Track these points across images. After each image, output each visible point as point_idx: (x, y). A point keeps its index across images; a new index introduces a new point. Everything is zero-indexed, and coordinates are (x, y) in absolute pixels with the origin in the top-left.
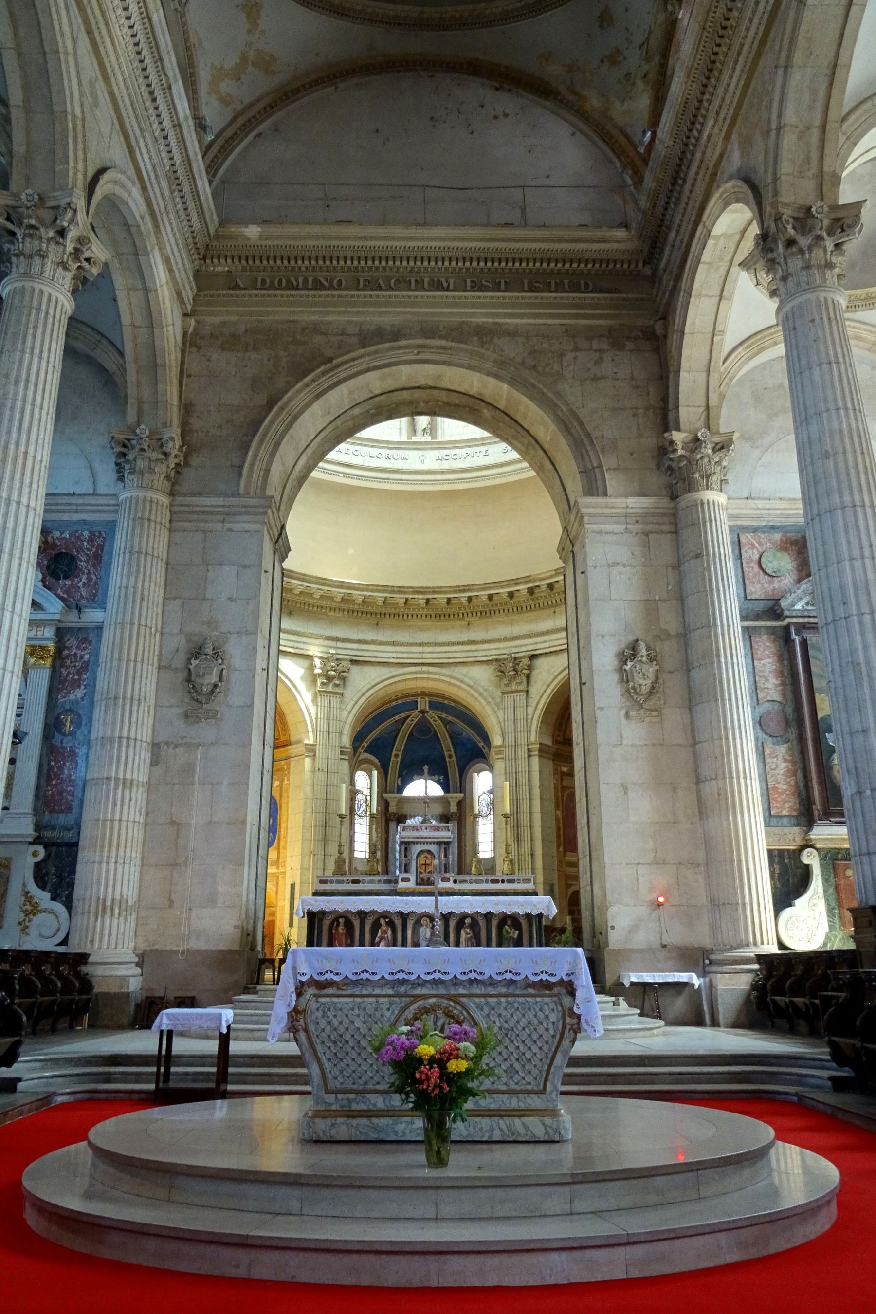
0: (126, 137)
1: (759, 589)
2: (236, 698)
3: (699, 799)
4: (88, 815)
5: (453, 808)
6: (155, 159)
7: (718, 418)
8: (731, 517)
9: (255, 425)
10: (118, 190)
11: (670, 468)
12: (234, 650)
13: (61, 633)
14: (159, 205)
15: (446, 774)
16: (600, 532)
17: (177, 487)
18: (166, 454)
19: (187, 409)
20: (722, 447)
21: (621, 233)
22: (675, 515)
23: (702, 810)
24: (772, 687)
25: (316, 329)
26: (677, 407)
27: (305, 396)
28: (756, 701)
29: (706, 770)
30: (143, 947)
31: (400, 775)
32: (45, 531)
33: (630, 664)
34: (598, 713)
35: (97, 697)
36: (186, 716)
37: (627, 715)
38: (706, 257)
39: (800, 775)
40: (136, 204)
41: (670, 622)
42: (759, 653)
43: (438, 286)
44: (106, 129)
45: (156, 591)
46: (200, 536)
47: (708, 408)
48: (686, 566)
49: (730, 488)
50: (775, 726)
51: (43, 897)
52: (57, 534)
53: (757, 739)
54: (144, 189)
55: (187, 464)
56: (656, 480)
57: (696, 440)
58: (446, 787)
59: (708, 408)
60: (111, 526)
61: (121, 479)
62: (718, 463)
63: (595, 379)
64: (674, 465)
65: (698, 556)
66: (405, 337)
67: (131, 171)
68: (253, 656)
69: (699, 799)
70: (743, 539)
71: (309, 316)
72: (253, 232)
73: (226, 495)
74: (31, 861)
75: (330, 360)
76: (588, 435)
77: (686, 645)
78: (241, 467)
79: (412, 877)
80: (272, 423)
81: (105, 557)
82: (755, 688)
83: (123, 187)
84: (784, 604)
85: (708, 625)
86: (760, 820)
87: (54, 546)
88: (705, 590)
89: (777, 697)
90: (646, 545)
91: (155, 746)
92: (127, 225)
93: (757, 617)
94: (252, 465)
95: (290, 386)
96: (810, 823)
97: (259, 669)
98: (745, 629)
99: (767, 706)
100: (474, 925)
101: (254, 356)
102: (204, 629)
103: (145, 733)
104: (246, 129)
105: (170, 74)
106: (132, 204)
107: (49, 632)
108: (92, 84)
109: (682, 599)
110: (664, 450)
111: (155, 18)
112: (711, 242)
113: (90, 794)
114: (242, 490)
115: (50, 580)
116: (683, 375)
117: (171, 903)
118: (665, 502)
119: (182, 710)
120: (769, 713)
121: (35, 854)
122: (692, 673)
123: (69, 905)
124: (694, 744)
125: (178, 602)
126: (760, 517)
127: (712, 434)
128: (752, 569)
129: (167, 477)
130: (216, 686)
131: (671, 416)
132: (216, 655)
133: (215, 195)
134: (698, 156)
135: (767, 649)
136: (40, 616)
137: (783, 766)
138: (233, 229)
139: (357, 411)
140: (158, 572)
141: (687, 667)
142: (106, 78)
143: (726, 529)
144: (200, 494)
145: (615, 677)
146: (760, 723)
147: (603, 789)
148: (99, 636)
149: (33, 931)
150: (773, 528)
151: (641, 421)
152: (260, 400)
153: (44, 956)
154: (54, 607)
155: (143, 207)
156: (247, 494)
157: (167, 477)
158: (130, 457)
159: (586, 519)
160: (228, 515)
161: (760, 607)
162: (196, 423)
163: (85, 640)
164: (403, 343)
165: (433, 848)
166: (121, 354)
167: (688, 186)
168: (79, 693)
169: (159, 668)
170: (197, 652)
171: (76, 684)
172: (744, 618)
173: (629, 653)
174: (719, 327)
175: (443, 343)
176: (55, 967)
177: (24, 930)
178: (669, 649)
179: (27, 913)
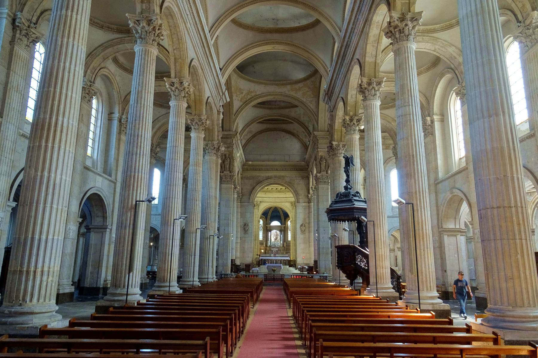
5: (283, 229)
9: (251, 192)
12: (250, 225)
15: (281, 221)
19: (242, 189)
21: (303, 162)
23: (309, 247)
25: (260, 176)
27: (258, 187)
31: (270, 220)
41: (307, 221)
43: (277, 170)
56: (307, 200)
58: (281, 224)
63: (299, 184)
72: (250, 163)
75: (261, 181)
80: (254, 192)
91: (240, 238)
100: (280, 261)
104: (248, 143)
110: (308, 196)
118: (307, 204)
138: (248, 162)
152: (252, 188)
162: (243, 191)
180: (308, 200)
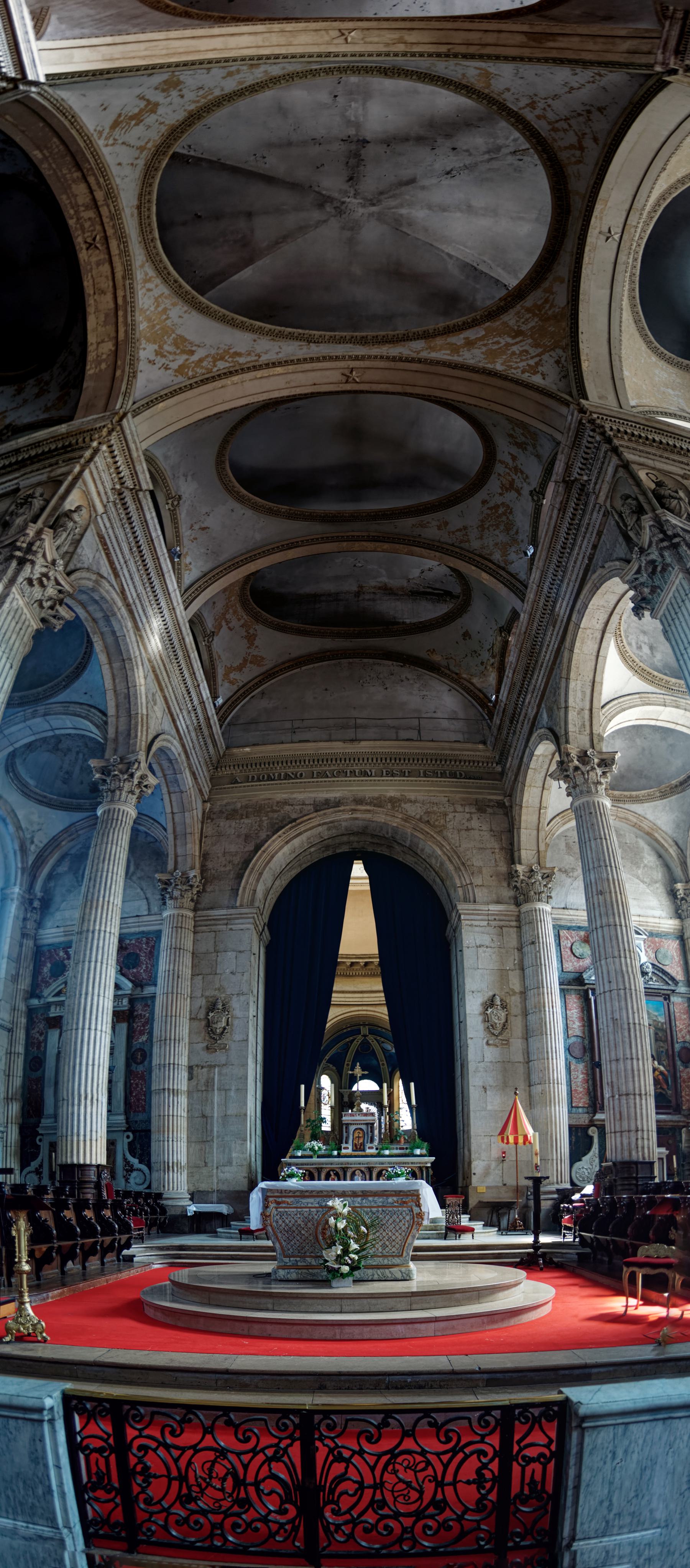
0: (172, 715)
1: (571, 965)
2: (237, 1037)
3: (530, 1095)
4: (154, 1113)
6: (188, 722)
7: (545, 857)
8: (554, 919)
10: (165, 744)
11: (516, 887)
13: (132, 1001)
14: (189, 745)
16: (471, 925)
17: (199, 906)
18: (192, 886)
20: (548, 877)
22: (519, 916)
24: (577, 1027)
26: (519, 850)
28: (567, 1036)
29: (534, 1078)
30: (192, 1189)
32: (121, 940)
33: (490, 1010)
34: (469, 1041)
35: (155, 1040)
36: (207, 1048)
37: (488, 1044)
38: (532, 765)
39: (590, 1082)
40: (176, 748)
42: (569, 1006)
44: (159, 714)
45: (187, 972)
46: (213, 934)
47: (538, 851)
48: (525, 949)
49: (553, 902)
50: (577, 1052)
51: (135, 1161)
52: (128, 942)
53: (566, 1059)
54: (181, 739)
55: (204, 890)
57: (532, 871)
59: (538, 851)
60: (158, 934)
61: (164, 904)
62: (545, 886)
64: (518, 885)
65: (533, 943)
66: (343, 804)
67: (174, 732)
68: (247, 1009)
69: (530, 1095)
70: (561, 933)
71: (281, 796)
73: (228, 908)
74: (126, 1141)
76: (463, 864)
77: (525, 999)
78: (238, 890)
79: (350, 1147)
81: (156, 953)
82: (567, 1028)
83: (169, 741)
84: (585, 976)
85: (539, 986)
86: (565, 1109)
87: (126, 948)
88: (538, 965)
89: (579, 1033)
90: (501, 935)
92: (170, 761)
93: (569, 984)
94: (245, 888)
95: (269, 837)
96: (595, 1113)
97: (251, 1017)
98: (562, 990)
99: (573, 1040)
101: (246, 821)
102: (216, 993)
103: (184, 1061)
105: (199, 679)
106: (173, 749)
107: (125, 1002)
108: (153, 695)
109: (522, 969)
110: (511, 875)
111: (192, 656)
112: (534, 758)
113: (155, 1100)
114: (238, 904)
115: (125, 970)
116: (523, 831)
117: (206, 1164)
119: (205, 1045)
120: (574, 1043)
121: (128, 1137)
122: (529, 1017)
123: (149, 1166)
124: (528, 1062)
125: (200, 977)
126: (571, 920)
127: (541, 868)
128: (567, 953)
129: (192, 900)
130: (224, 1029)
131: (516, 854)
132: (224, 1008)
133: (223, 734)
134: (524, 711)
135: (574, 1002)
136: (120, 993)
137: (581, 1076)
139: (312, 850)
140: (188, 960)
141: (525, 1014)
142: (162, 690)
143: (551, 927)
144: (212, 908)
145: (480, 1018)
146: (569, 1050)
147: (471, 1089)
148: (153, 1002)
149: (132, 1181)
150: (580, 928)
151: (497, 856)
153: (138, 1194)
154: (128, 985)
155: (180, 749)
156: (241, 906)
157: (192, 900)
158: (170, 890)
159: (462, 917)
160: (228, 920)
161: (572, 976)
163: (147, 1005)
164: (342, 808)
165: (364, 1127)
166: (165, 830)
167: (519, 726)
168: (144, 1038)
169: (191, 1019)
170: (212, 1007)
171: (142, 1033)
172: (561, 984)
173: (490, 1003)
174: (544, 805)
175: (368, 808)
176: (145, 1200)
177: (127, 1180)
178: (515, 1002)
179: (127, 1171)
180: (512, 893)
